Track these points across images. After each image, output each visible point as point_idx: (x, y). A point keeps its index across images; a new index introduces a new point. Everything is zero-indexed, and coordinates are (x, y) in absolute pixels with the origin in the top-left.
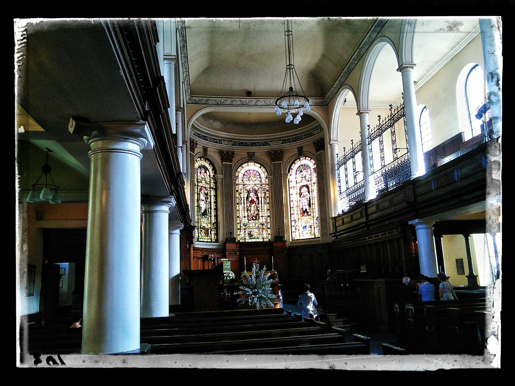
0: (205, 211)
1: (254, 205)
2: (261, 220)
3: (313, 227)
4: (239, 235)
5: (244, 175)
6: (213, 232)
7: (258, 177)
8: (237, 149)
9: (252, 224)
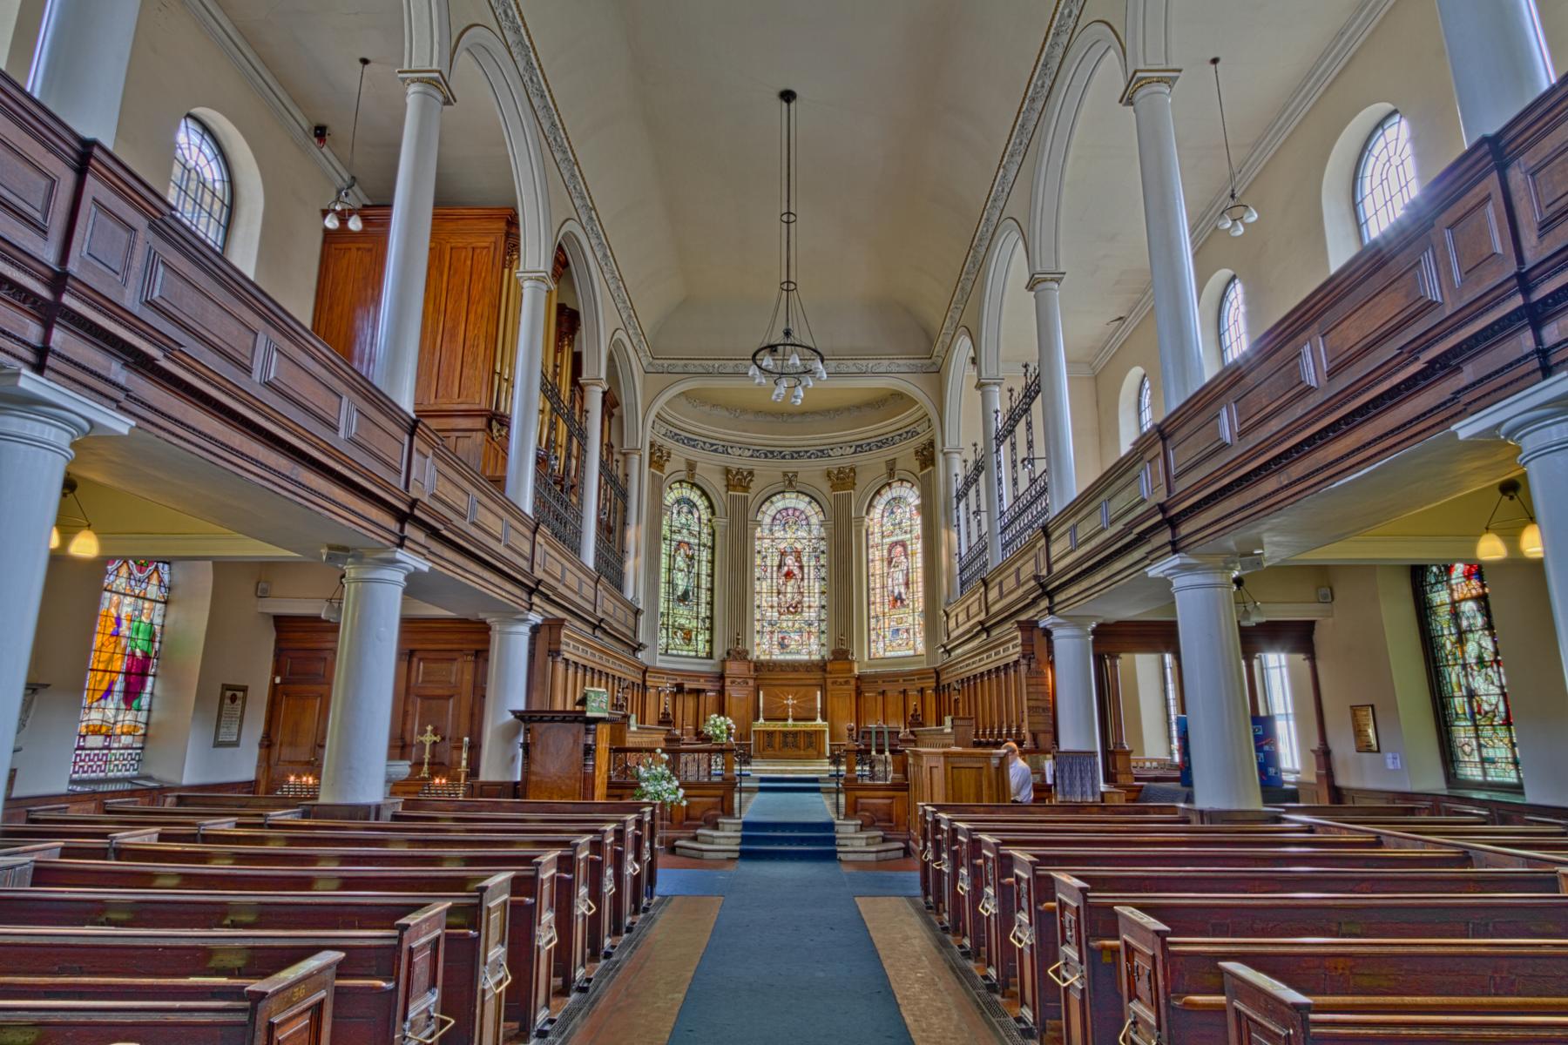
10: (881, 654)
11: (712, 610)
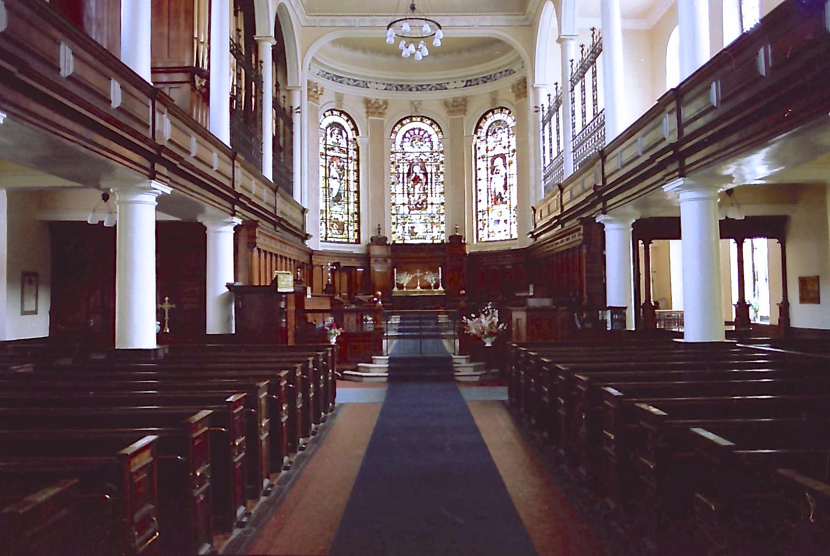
0: (339, 195)
1: (419, 185)
2: (429, 210)
3: (508, 222)
4: (394, 233)
5: (404, 137)
6: (350, 228)
7: (427, 140)
8: (392, 96)
9: (415, 217)
10: (486, 239)
11: (358, 207)
